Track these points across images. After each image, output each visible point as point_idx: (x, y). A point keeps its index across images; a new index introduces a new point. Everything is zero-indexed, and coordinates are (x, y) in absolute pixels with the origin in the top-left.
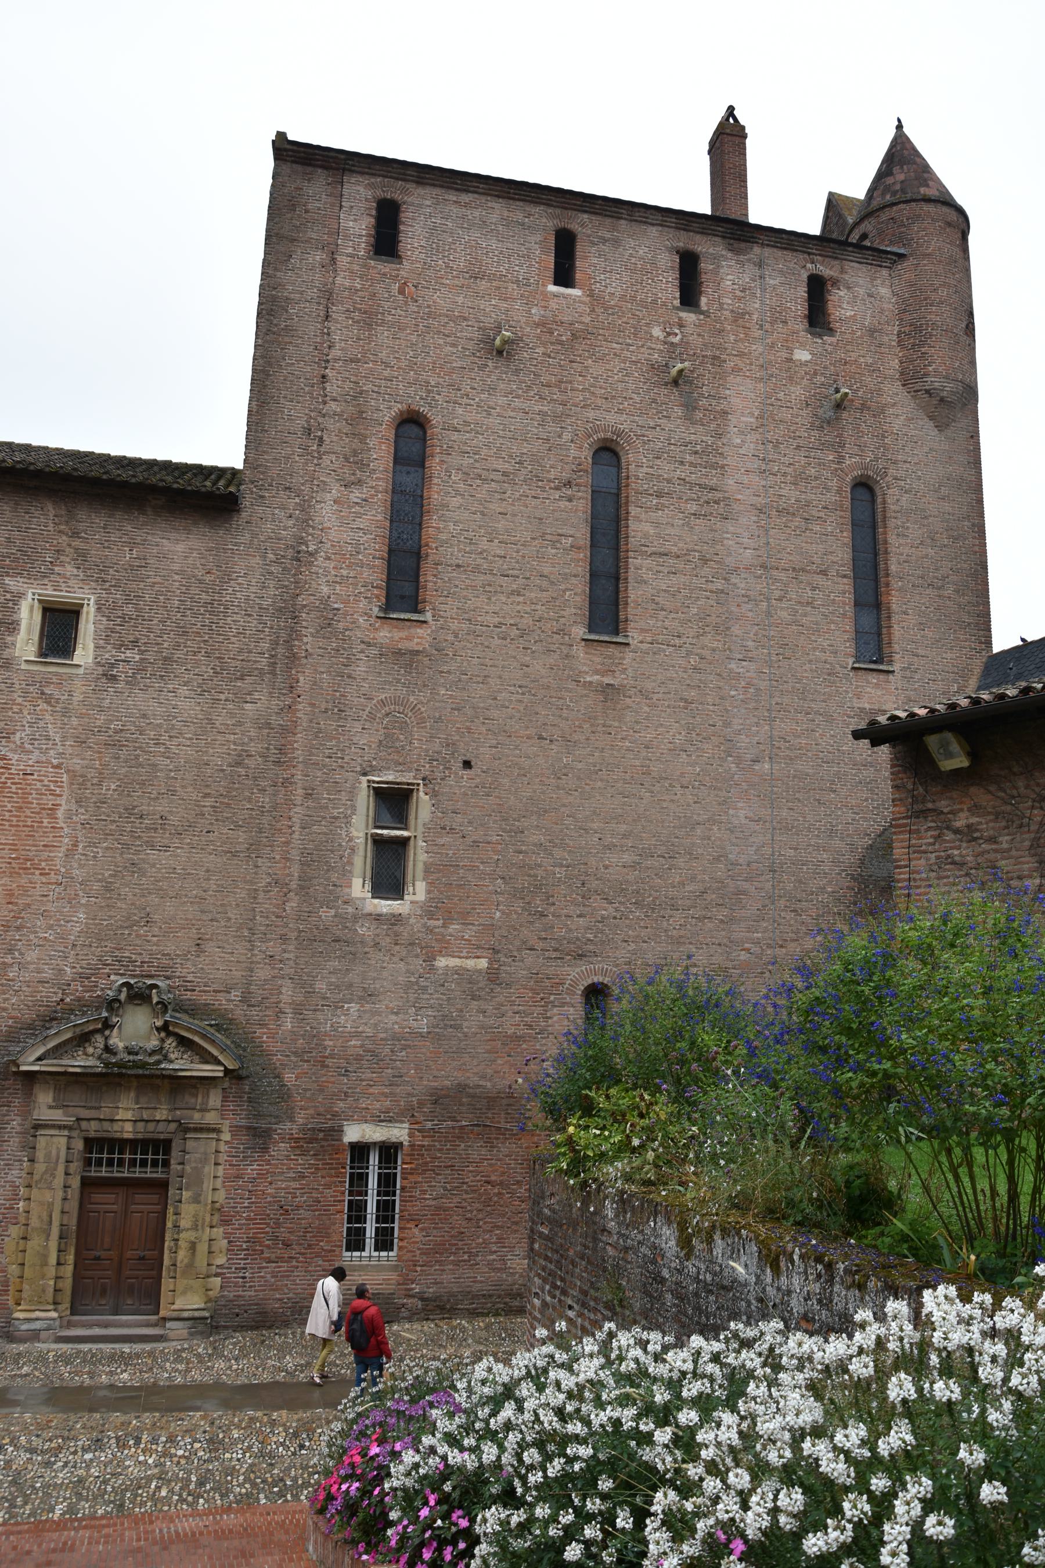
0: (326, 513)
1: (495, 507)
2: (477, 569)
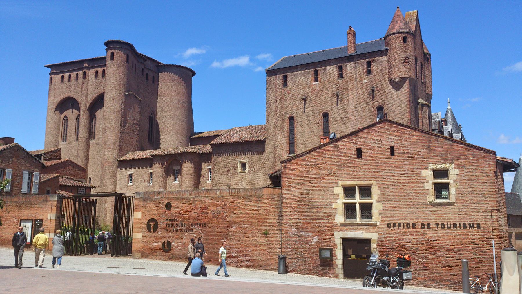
0: (279, 139)
1: (306, 131)
2: (303, 144)
